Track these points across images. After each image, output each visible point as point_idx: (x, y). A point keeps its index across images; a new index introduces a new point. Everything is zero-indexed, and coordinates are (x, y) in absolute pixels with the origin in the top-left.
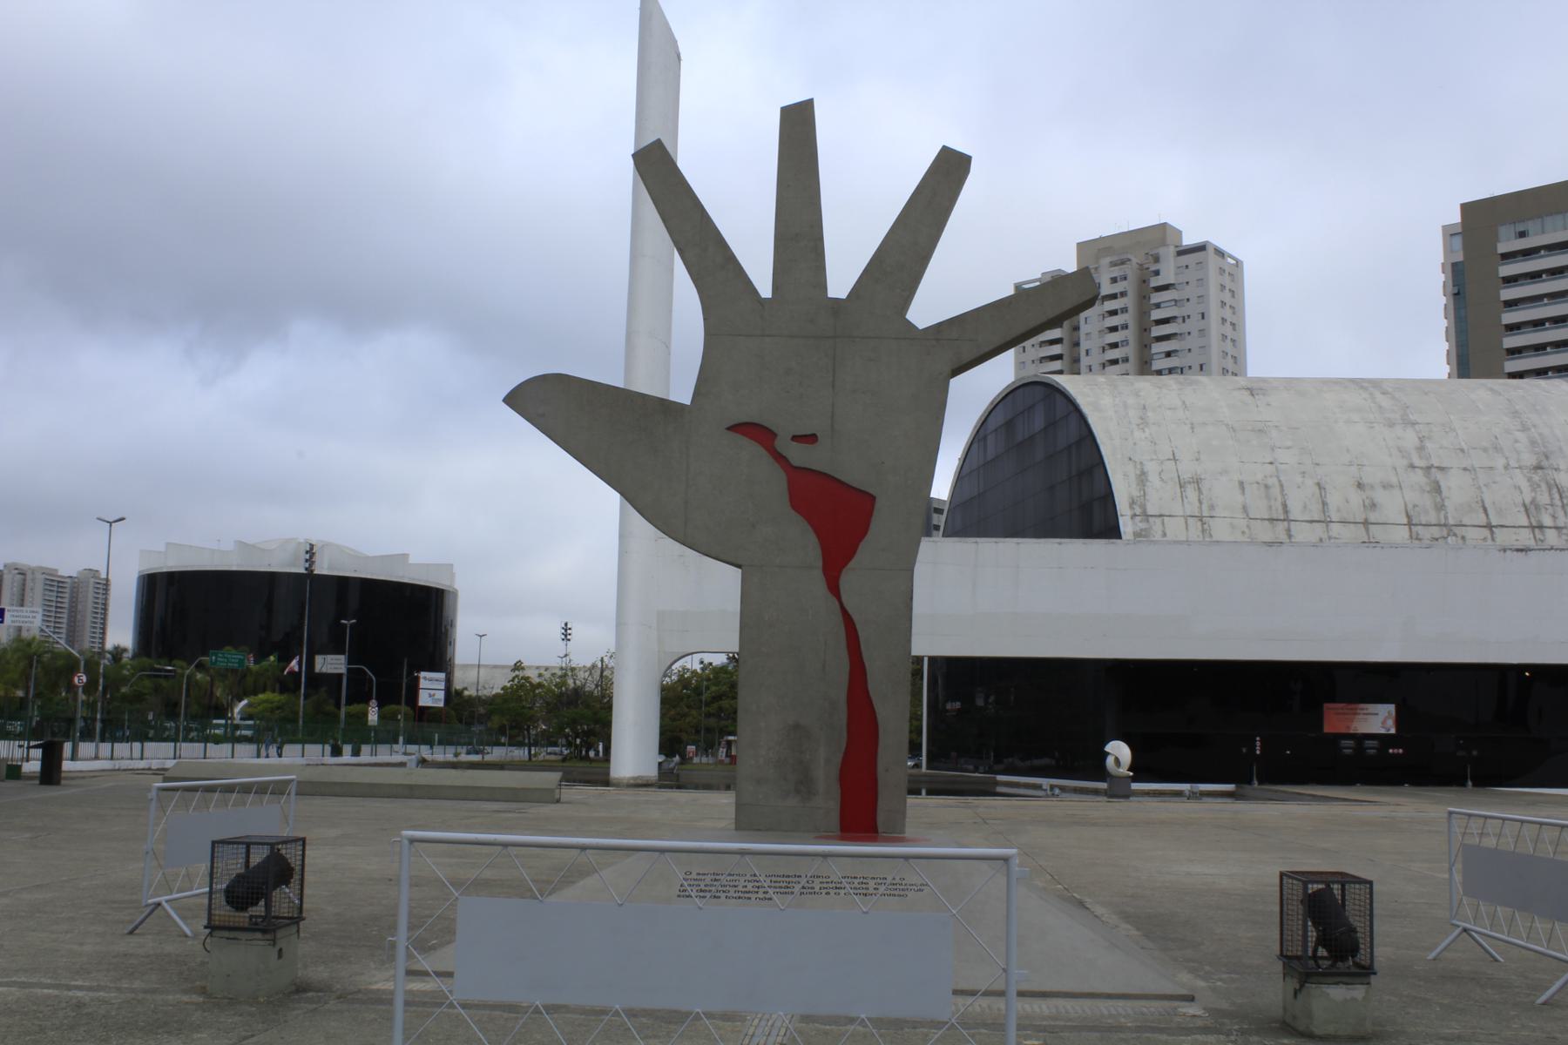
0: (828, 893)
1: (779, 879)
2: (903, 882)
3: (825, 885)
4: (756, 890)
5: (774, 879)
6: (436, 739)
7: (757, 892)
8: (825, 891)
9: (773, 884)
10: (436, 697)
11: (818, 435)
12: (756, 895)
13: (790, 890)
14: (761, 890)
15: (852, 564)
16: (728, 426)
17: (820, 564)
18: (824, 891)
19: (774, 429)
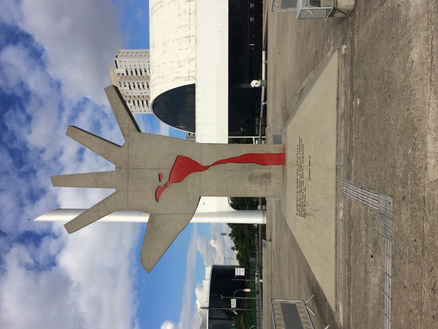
0: (303, 170)
1: (298, 185)
2: (299, 145)
3: (300, 170)
4: (302, 192)
5: (298, 187)
6: (254, 270)
7: (303, 192)
8: (302, 170)
9: (300, 187)
10: (242, 271)
12: (304, 193)
13: (302, 182)
14: (302, 191)
15: (199, 162)
17: (199, 172)
18: (302, 171)
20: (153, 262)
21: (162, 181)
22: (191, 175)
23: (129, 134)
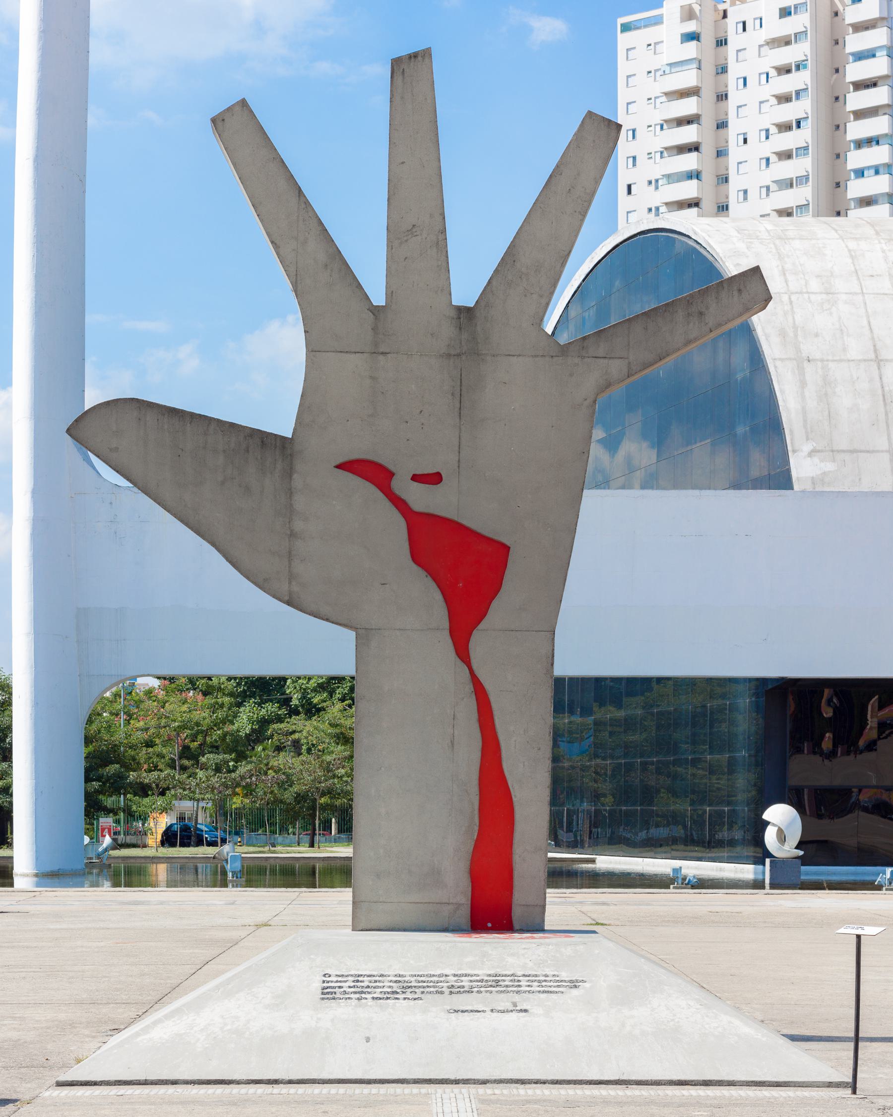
11: (443, 475)
15: (482, 626)
16: (338, 463)
17: (447, 625)
19: (391, 467)
20: (111, 450)
21: (416, 484)
22: (438, 596)
23: (589, 360)
